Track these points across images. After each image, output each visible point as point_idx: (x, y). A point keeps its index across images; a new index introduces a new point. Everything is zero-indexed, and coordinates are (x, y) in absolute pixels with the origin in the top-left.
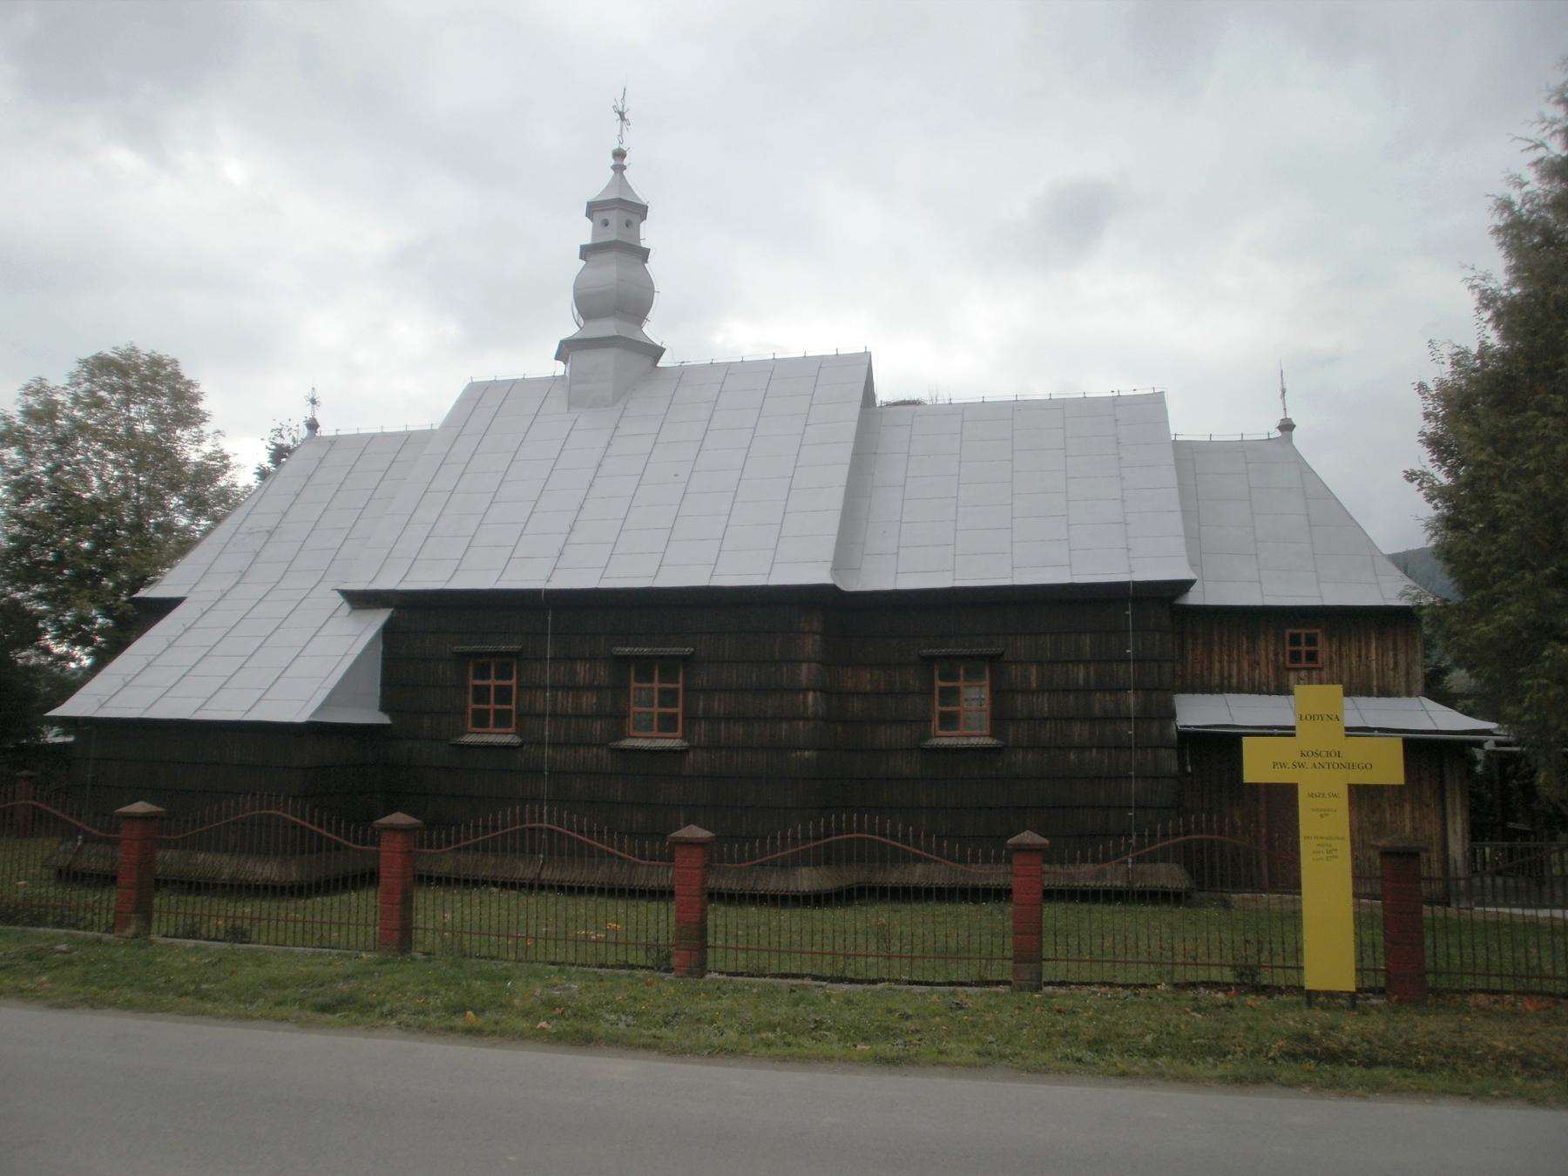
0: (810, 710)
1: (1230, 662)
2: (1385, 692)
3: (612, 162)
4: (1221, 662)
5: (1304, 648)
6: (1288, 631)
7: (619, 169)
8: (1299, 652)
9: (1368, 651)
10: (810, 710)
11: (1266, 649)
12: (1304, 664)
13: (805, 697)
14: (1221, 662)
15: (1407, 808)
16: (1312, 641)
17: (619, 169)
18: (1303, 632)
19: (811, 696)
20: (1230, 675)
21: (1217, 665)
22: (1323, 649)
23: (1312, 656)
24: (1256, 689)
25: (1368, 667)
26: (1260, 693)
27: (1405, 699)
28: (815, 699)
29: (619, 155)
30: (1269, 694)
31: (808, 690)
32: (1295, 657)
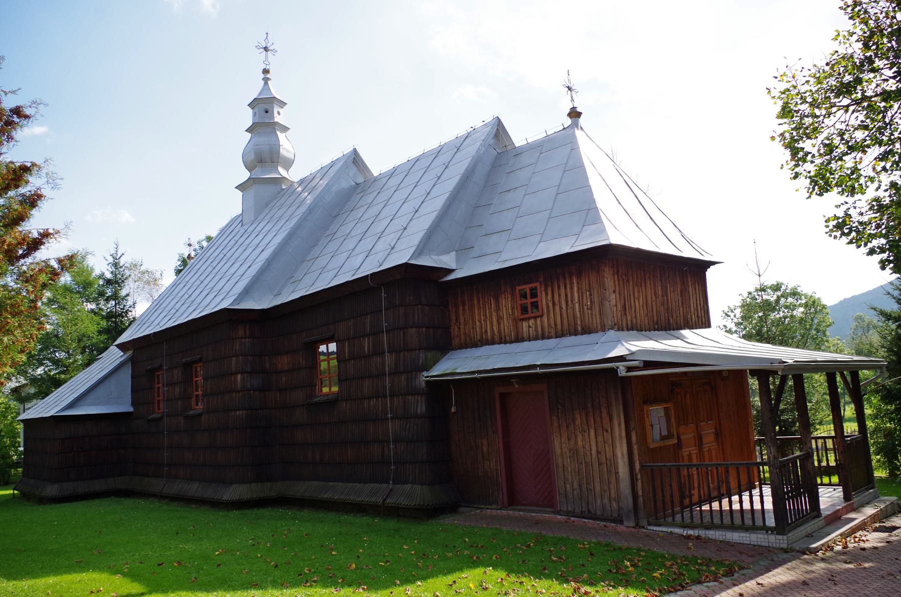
0: (239, 385)
1: (485, 321)
3: (263, 76)
5: (529, 300)
6: (518, 288)
7: (266, 80)
8: (532, 303)
9: (572, 295)
10: (239, 385)
11: (507, 305)
13: (236, 379)
16: (534, 295)
17: (266, 80)
18: (527, 288)
19: (239, 376)
20: (486, 331)
22: (544, 299)
23: (535, 305)
24: (503, 341)
25: (574, 309)
26: (506, 343)
27: (600, 334)
28: (243, 380)
29: (266, 71)
30: (511, 342)
31: (238, 374)
32: (524, 310)
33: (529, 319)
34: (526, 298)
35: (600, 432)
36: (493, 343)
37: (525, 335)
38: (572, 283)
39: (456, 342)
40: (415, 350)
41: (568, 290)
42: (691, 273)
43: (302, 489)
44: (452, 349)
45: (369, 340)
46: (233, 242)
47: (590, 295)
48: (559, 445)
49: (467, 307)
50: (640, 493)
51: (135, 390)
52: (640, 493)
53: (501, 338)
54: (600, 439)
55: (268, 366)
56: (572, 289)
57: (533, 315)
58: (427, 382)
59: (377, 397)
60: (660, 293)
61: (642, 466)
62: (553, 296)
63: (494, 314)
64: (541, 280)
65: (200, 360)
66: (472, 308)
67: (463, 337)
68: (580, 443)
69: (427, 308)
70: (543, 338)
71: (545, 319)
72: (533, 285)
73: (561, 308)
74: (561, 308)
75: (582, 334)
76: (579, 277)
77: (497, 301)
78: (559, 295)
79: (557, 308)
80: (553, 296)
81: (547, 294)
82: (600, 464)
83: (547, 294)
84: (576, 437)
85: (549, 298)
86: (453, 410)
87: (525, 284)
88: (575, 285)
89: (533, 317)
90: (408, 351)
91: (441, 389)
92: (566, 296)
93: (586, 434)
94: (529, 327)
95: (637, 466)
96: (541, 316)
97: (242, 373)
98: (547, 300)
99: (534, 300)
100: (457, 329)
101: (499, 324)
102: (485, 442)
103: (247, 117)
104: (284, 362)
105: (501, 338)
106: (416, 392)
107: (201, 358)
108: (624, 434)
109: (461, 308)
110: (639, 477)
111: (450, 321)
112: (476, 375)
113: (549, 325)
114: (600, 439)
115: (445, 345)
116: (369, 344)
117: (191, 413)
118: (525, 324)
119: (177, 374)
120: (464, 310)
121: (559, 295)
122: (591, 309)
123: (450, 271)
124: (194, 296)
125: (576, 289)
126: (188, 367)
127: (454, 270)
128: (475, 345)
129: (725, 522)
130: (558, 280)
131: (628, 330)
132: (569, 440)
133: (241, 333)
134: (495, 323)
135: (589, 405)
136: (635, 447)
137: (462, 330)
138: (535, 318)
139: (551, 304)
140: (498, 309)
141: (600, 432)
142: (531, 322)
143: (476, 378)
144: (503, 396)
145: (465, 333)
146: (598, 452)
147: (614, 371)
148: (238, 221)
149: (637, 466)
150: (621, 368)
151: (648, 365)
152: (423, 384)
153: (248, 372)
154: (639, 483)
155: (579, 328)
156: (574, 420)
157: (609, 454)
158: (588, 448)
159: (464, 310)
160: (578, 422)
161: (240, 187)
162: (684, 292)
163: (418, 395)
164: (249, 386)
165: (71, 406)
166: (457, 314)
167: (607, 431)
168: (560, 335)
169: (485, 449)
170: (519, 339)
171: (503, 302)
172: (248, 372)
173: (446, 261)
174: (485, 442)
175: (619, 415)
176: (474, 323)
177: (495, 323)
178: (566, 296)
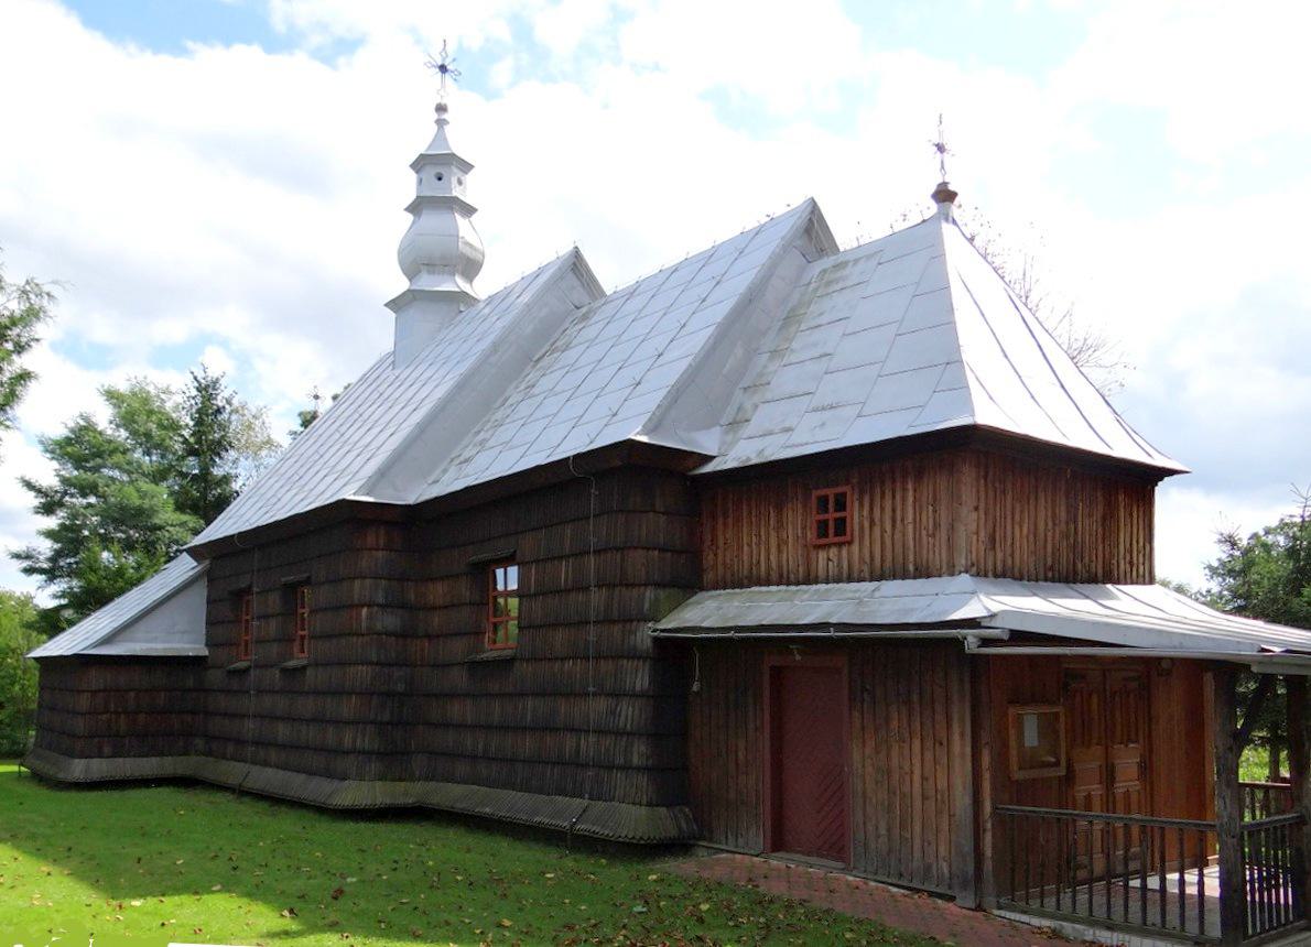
0: (364, 625)
1: (758, 545)
2: (923, 572)
4: (750, 545)
5: (832, 515)
6: (816, 493)
11: (797, 522)
12: (832, 539)
14: (750, 545)
15: (917, 744)
16: (841, 504)
18: (831, 492)
19: (365, 610)
20: (759, 562)
21: (746, 548)
22: (856, 515)
23: (841, 527)
24: (783, 579)
27: (945, 579)
28: (370, 617)
30: (798, 583)
31: (363, 606)
32: (822, 529)
33: (829, 546)
34: (826, 511)
35: (929, 744)
36: (768, 583)
37: (821, 573)
38: (905, 490)
39: (709, 577)
40: (640, 585)
41: (898, 497)
42: (1127, 487)
43: (233, 771)
44: (702, 589)
45: (567, 566)
46: (375, 395)
47: (935, 511)
48: (861, 760)
49: (730, 520)
50: (988, 852)
51: (212, 622)
52: (988, 852)
53: (781, 576)
54: (929, 755)
55: (413, 597)
56: (904, 500)
57: (837, 539)
58: (655, 639)
59: (575, 658)
60: (1063, 515)
61: (995, 808)
62: (871, 509)
63: (773, 534)
64: (855, 481)
65: (307, 582)
66: (738, 520)
67: (720, 568)
68: (895, 761)
69: (663, 518)
70: (850, 580)
71: (855, 547)
72: (840, 490)
73: (883, 531)
74: (883, 531)
75: (915, 578)
76: (919, 477)
77: (779, 509)
78: (882, 509)
79: (877, 531)
80: (871, 509)
81: (861, 505)
82: (924, 798)
83: (861, 505)
84: (889, 749)
85: (866, 513)
86: (696, 687)
87: (828, 486)
88: (911, 493)
89: (835, 544)
90: (627, 585)
91: (677, 652)
92: (894, 511)
93: (906, 746)
94: (829, 559)
95: (988, 807)
96: (850, 543)
97: (369, 606)
98: (861, 516)
99: (839, 515)
100: (711, 556)
101: (780, 551)
102: (742, 744)
103: (408, 187)
104: (437, 592)
105: (781, 576)
106: (634, 655)
107: (309, 578)
108: (968, 750)
109: (721, 521)
110: (989, 825)
111: (702, 541)
112: (731, 634)
113: (861, 559)
114: (929, 755)
115: (690, 582)
116: (567, 572)
117: (291, 664)
118: (822, 555)
119: (274, 601)
120: (725, 524)
121: (882, 509)
122: (934, 536)
123: (708, 459)
124: (306, 478)
125: (911, 499)
126: (291, 591)
127: (712, 458)
128: (739, 584)
129: (1150, 919)
130: (883, 483)
131: (996, 576)
132: (878, 753)
133: (370, 540)
134: (774, 550)
135: (915, 698)
136: (987, 776)
137: (720, 558)
138: (840, 545)
139: (867, 524)
140: (780, 525)
141: (929, 744)
142: (833, 551)
143: (731, 639)
144: (777, 673)
145: (724, 563)
146: (924, 778)
147: (958, 643)
148: (394, 359)
149: (988, 807)
150: (971, 638)
151: (1018, 637)
152: (648, 643)
153: (378, 605)
154: (988, 838)
155: (911, 568)
156: (887, 721)
157: (942, 783)
158: (907, 768)
159: (725, 524)
160: (895, 723)
161: (394, 305)
162: (1109, 517)
163: (639, 658)
164: (379, 626)
165: (108, 640)
166: (714, 529)
167: (941, 744)
168: (879, 576)
169: (741, 755)
170: (810, 579)
171: (789, 515)
172: (378, 605)
173: (705, 442)
174: (742, 744)
175: (962, 720)
176: (740, 548)
177: (774, 550)
178: (894, 511)
